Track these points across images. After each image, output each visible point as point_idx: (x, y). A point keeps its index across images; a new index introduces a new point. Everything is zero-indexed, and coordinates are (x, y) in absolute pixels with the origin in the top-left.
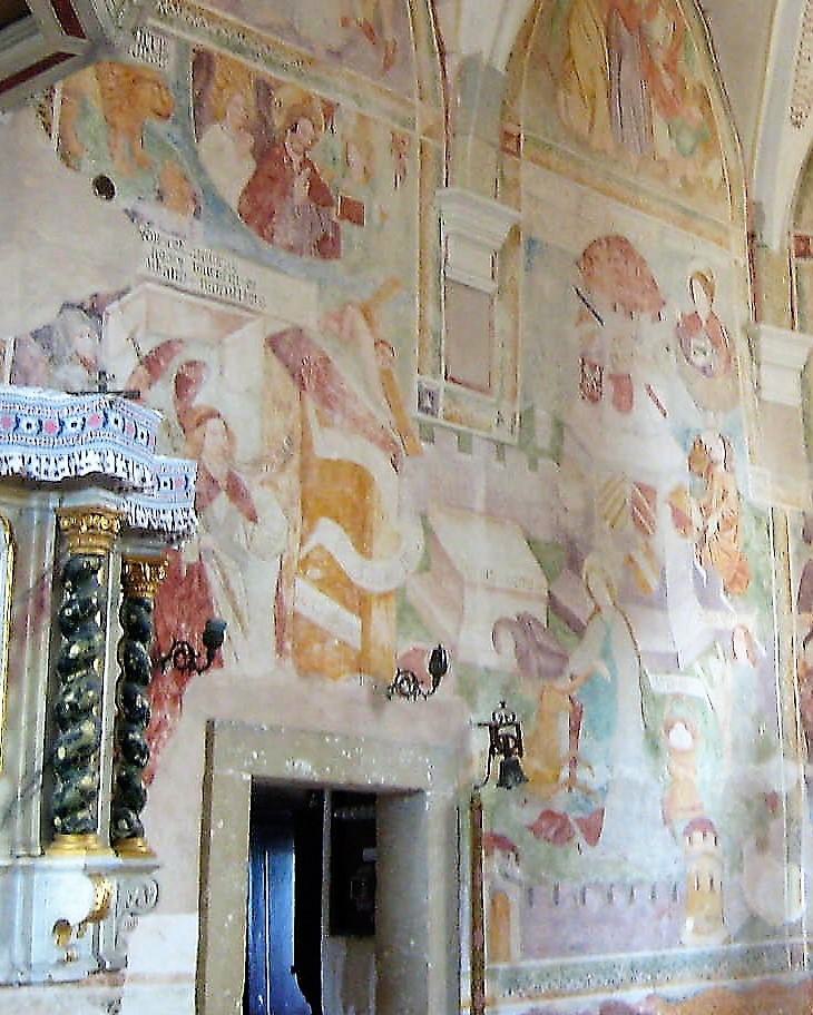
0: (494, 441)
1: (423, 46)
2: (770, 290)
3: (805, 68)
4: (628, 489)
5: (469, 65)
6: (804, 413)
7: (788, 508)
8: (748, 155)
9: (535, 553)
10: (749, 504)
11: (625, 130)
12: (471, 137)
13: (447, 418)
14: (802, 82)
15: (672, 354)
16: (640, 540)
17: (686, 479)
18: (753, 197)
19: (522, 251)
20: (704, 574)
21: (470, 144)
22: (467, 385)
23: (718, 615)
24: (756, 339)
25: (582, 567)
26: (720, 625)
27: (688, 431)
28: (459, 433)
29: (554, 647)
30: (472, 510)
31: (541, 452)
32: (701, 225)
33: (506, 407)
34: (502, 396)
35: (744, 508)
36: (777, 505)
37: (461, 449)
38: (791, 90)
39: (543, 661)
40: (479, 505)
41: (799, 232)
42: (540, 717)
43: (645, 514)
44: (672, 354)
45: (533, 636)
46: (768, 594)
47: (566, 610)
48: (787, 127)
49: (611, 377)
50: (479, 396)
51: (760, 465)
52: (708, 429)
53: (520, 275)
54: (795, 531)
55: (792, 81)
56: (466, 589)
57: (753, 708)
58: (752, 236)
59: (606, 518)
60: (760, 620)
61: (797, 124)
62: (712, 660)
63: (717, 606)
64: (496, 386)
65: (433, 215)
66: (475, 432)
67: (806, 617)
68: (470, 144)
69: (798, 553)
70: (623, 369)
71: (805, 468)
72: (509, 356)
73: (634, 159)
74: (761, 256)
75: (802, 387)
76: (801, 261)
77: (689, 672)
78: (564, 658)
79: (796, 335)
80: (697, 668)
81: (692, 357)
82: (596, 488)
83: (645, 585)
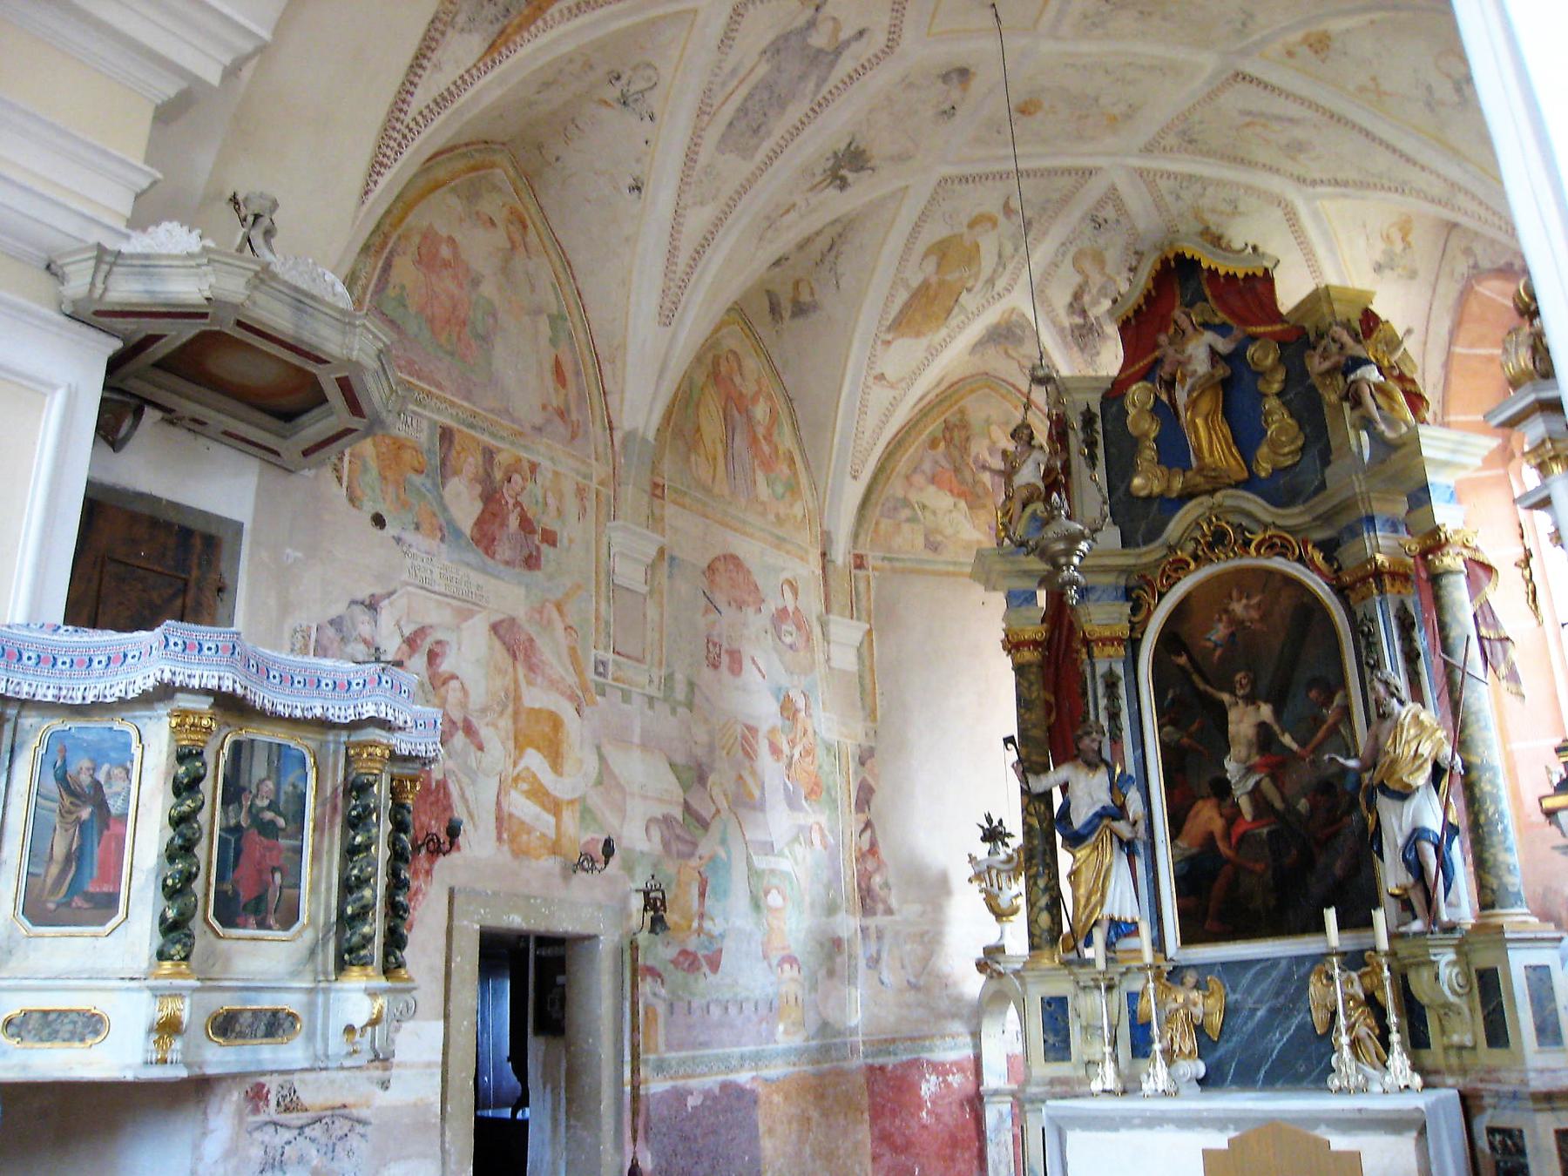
1: (598, 423)
4: (739, 729)
5: (630, 436)
7: (849, 742)
8: (821, 500)
10: (822, 739)
13: (615, 679)
14: (859, 448)
15: (769, 636)
16: (747, 762)
17: (779, 722)
18: (825, 527)
19: (666, 564)
22: (628, 657)
23: (801, 815)
26: (802, 822)
28: (622, 690)
29: (688, 837)
30: (631, 743)
31: (680, 703)
32: (789, 547)
35: (819, 741)
40: (636, 739)
42: (679, 885)
43: (751, 746)
46: (835, 801)
48: (848, 479)
49: (727, 651)
50: (636, 664)
53: (665, 582)
54: (853, 757)
56: (628, 798)
58: (824, 555)
59: (723, 748)
61: (855, 477)
62: (797, 846)
63: (800, 809)
64: (648, 657)
65: (605, 540)
66: (634, 689)
69: (856, 773)
70: (735, 646)
72: (657, 636)
74: (830, 567)
77: (781, 854)
78: (695, 845)
79: (854, 623)
80: (786, 851)
83: (750, 795)
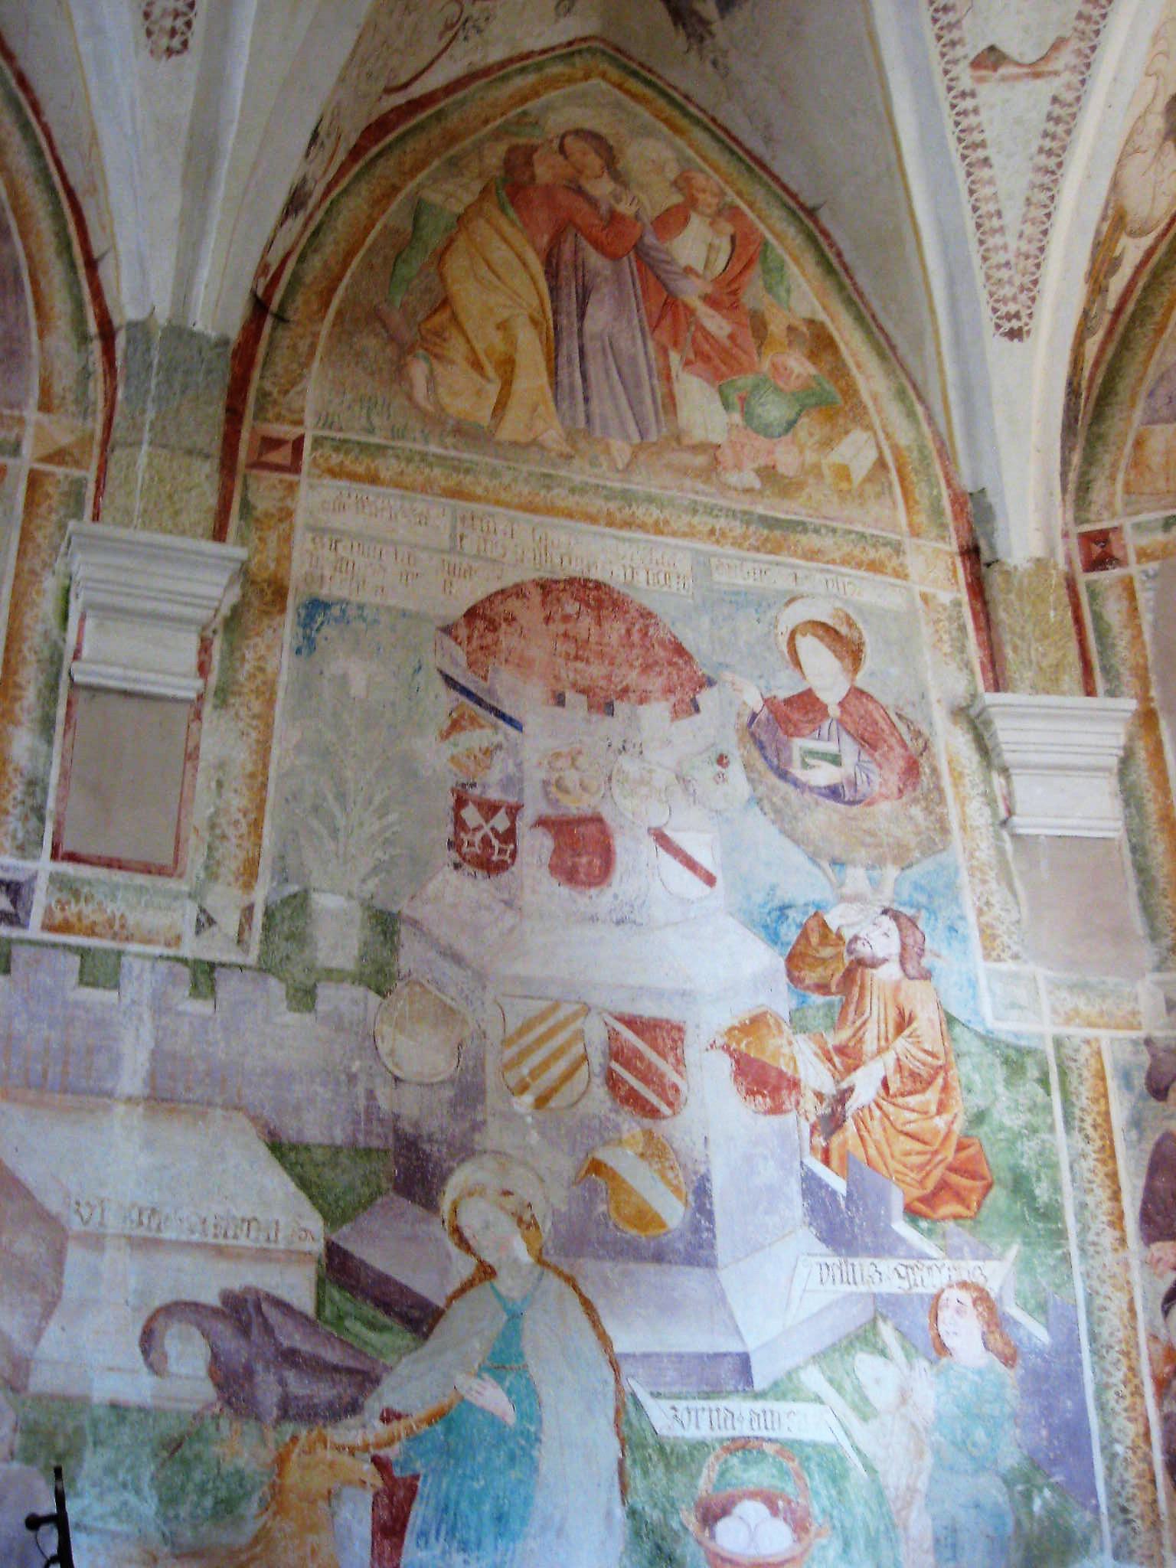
0: (184, 961)
1: (62, 325)
2: (1022, 637)
3: (994, 231)
4: (596, 1033)
5: (140, 329)
6: (1134, 849)
7: (1104, 1035)
8: (940, 420)
9: (289, 1167)
10: (989, 1041)
11: (595, 403)
12: (145, 447)
13: (49, 927)
14: (1001, 257)
15: (736, 771)
16: (630, 1125)
17: (781, 1001)
18: (966, 483)
19: (288, 627)
20: (839, 1185)
21: (143, 460)
22: (111, 864)
23: (886, 1265)
24: (988, 723)
25: (441, 1191)
26: (892, 1285)
27: (783, 909)
28: (84, 953)
29: (332, 1355)
30: (110, 1094)
31: (332, 975)
32: (809, 541)
33: (226, 903)
34: (212, 873)
35: (967, 1042)
36: (1077, 1032)
37: (87, 979)
38: (980, 279)
39: (298, 1385)
40: (131, 1079)
41: (1087, 528)
42: (276, 1499)
43: (648, 1076)
44: (736, 771)
45: (268, 1329)
46: (1050, 1214)
47: (385, 1280)
48: (996, 346)
49: (542, 822)
50: (161, 882)
51: (1016, 957)
52: (843, 899)
53: (284, 665)
54: (1126, 1078)
55: (976, 260)
56: (75, 1255)
57: (1011, 1457)
58: (971, 553)
59: (523, 1088)
60: (1025, 1266)
61: (1014, 334)
62: (865, 1364)
63: (883, 1245)
64: (195, 859)
65: (50, 584)
66: (134, 947)
67: (1163, 1249)
68: (143, 460)
69: (1137, 1122)
70: (575, 805)
71: (1147, 954)
72: (237, 801)
73: (620, 450)
74: (995, 580)
75: (1127, 804)
76: (1094, 576)
77: (783, 1389)
78: (367, 1379)
79: (1101, 701)
80: (813, 1379)
81: (797, 771)
82: (495, 1033)
83: (646, 1218)
